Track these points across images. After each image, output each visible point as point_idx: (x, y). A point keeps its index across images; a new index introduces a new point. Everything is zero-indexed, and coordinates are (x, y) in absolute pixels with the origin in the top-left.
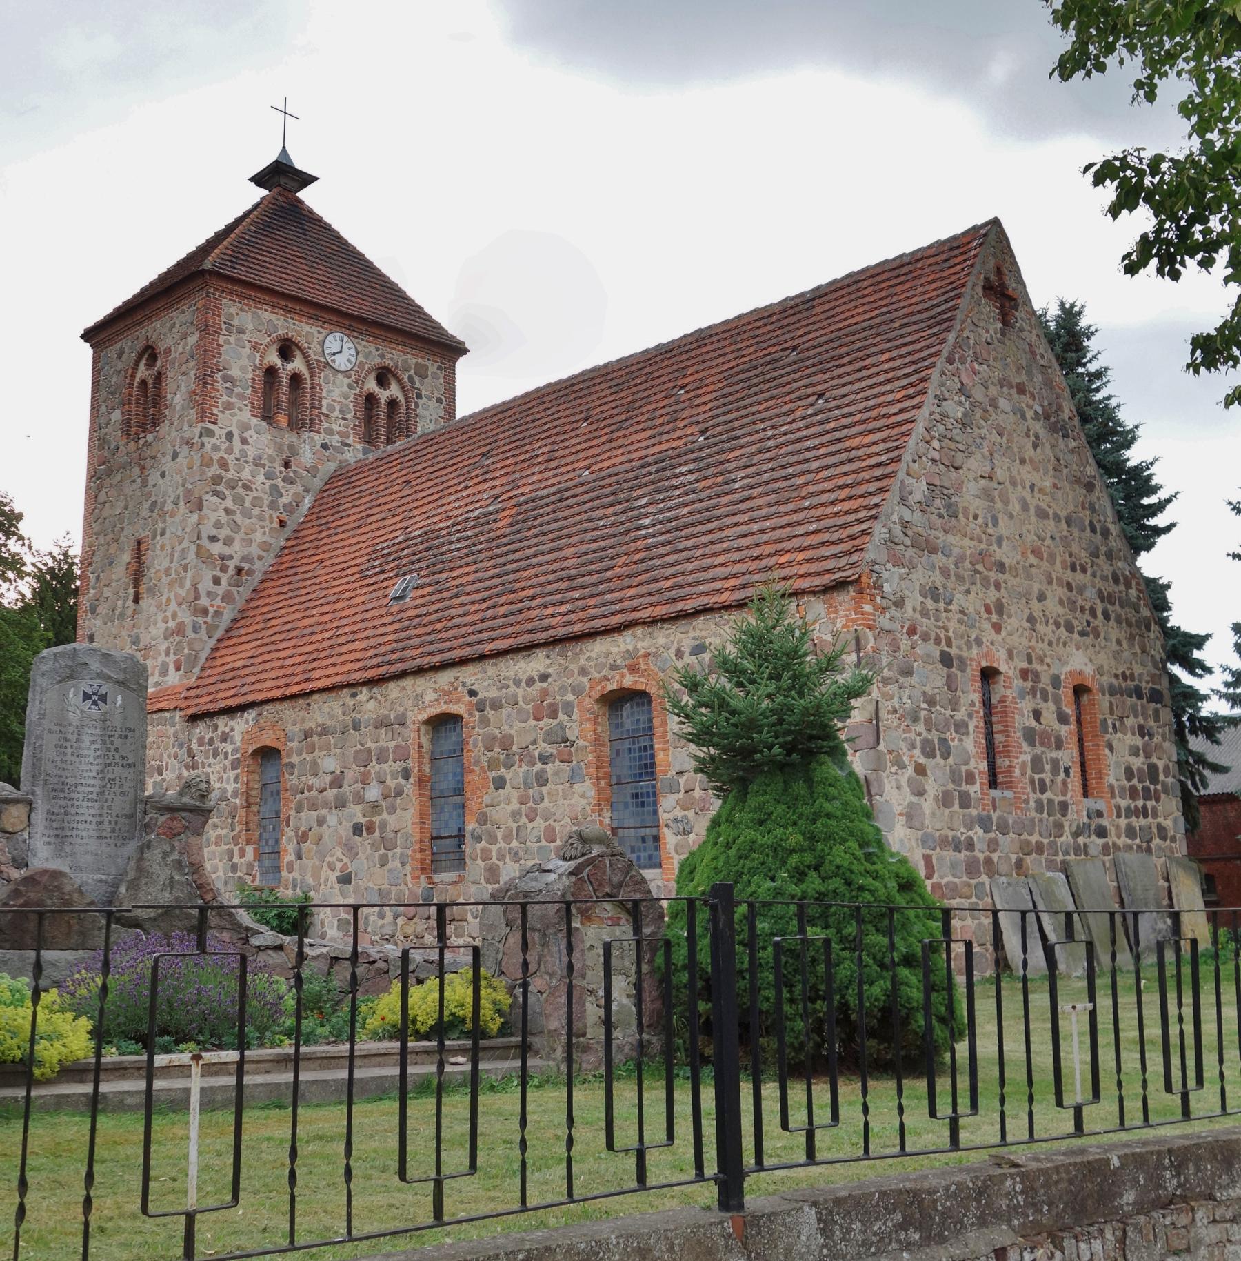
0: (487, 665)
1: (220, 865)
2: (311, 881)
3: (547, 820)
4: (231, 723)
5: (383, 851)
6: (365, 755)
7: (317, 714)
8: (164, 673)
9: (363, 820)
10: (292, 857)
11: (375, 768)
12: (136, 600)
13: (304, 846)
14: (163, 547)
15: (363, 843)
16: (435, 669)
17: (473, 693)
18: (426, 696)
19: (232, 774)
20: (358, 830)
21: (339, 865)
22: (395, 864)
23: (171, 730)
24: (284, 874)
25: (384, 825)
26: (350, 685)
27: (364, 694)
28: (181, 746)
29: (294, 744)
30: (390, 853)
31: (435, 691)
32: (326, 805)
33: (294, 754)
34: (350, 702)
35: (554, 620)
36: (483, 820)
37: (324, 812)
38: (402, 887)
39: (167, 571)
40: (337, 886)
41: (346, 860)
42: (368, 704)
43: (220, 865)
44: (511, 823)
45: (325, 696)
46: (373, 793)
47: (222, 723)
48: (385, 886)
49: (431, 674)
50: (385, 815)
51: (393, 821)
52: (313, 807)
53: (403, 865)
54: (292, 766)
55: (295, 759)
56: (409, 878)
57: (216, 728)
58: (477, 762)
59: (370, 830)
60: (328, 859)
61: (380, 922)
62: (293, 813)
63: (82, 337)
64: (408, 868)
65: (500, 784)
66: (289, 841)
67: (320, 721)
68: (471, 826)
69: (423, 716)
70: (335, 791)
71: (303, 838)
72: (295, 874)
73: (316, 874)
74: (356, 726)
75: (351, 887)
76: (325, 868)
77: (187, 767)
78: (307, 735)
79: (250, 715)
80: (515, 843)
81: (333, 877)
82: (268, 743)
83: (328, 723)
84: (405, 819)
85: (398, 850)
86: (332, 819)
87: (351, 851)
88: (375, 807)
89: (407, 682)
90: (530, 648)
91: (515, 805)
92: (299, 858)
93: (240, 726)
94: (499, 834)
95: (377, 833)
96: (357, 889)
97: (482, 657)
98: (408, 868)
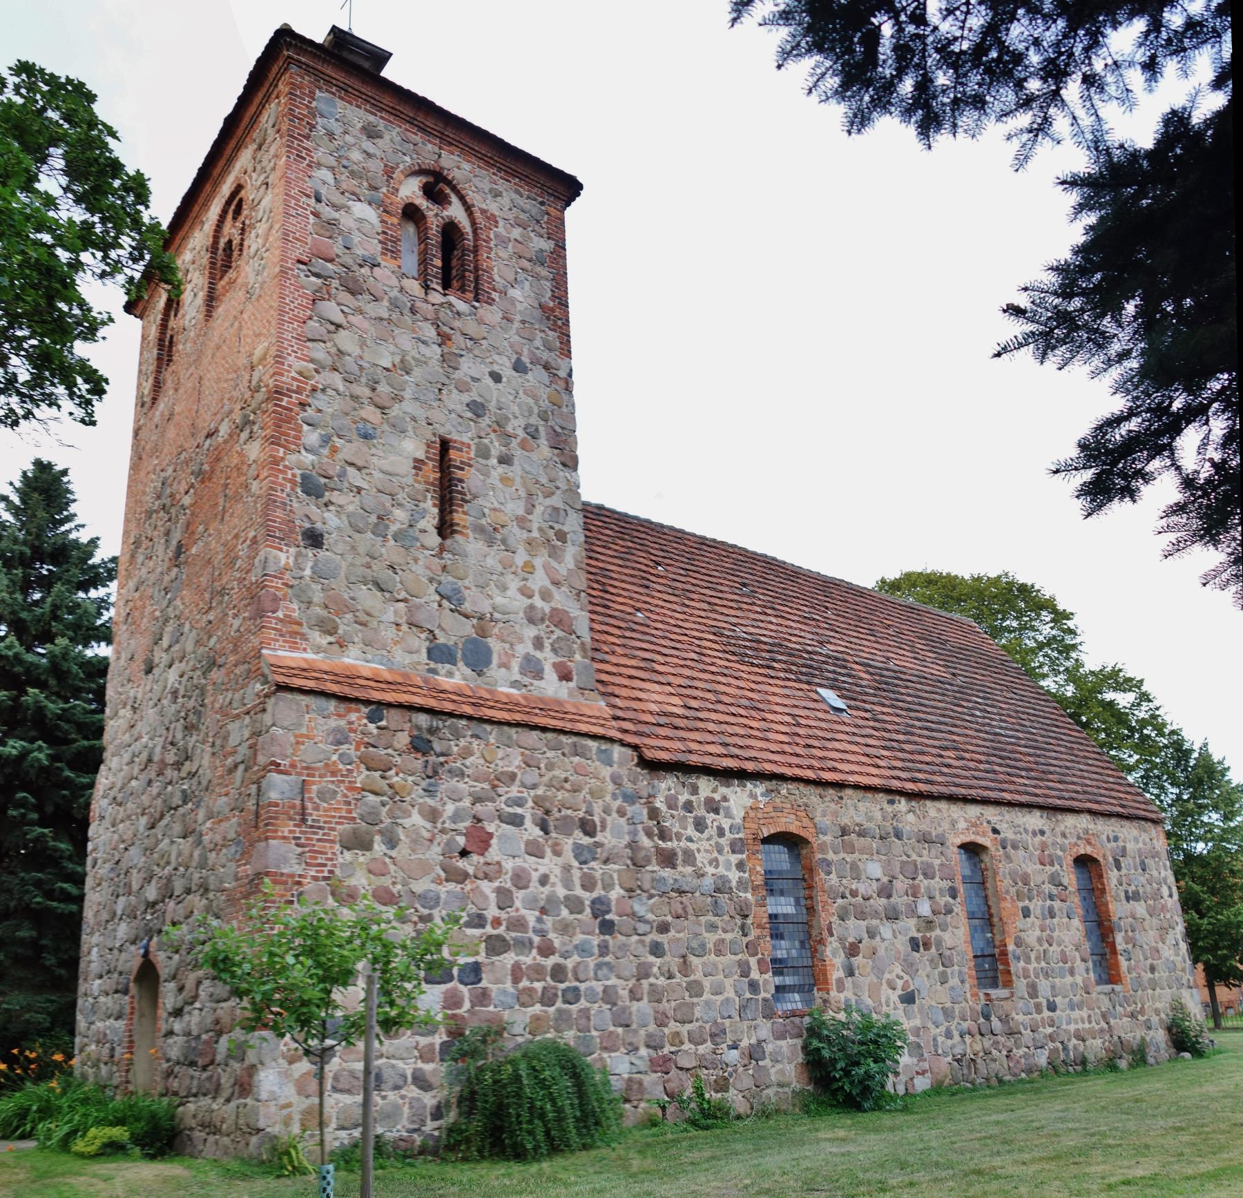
0: (1004, 809)
1: (728, 983)
2: (869, 1002)
3: (1059, 945)
4: (723, 790)
5: (941, 968)
6: (912, 867)
7: (852, 811)
8: (533, 669)
9: (919, 935)
10: (841, 974)
11: (922, 882)
12: (445, 528)
13: (858, 961)
14: (505, 480)
15: (922, 958)
16: (966, 800)
17: (995, 831)
18: (960, 823)
19: (734, 859)
20: (915, 944)
21: (900, 983)
22: (954, 982)
23: (606, 772)
24: (833, 993)
25: (939, 943)
26: (888, 791)
27: (902, 805)
28: (630, 799)
29: (828, 838)
30: (949, 970)
31: (966, 820)
32: (876, 914)
33: (825, 845)
34: (889, 808)
35: (1042, 794)
36: (1019, 943)
37: (875, 922)
38: (964, 1004)
39: (522, 522)
40: (901, 1006)
41: (906, 977)
42: (907, 815)
43: (728, 983)
44: (1038, 947)
45: (860, 794)
46: (925, 908)
47: (706, 786)
48: (948, 1005)
49: (961, 805)
50: (938, 932)
51: (948, 938)
52: (861, 915)
53: (963, 982)
54: (829, 864)
55: (831, 856)
56: (968, 995)
57: (695, 790)
58: (1007, 892)
59: (927, 945)
60: (887, 976)
61: (949, 1042)
62: (834, 919)
63: (334, 27)
64: (967, 985)
65: (1026, 913)
66: (834, 955)
67: (858, 820)
68: (1011, 947)
69: (958, 841)
70: (883, 901)
71: (853, 950)
72: (848, 994)
73: (874, 991)
74: (898, 835)
75: (915, 1007)
76: (885, 986)
77: (649, 834)
78: (844, 831)
79: (760, 788)
80: (1043, 964)
81: (894, 996)
82: (793, 829)
83: (867, 825)
84: (957, 936)
85: (956, 967)
86: (886, 930)
87: (910, 968)
88: (929, 924)
89: (943, 805)
90: (1029, 806)
91: (1038, 933)
92: (851, 973)
93: (739, 798)
94: (1033, 955)
95: (933, 950)
96: (921, 1010)
97: (1010, 804)
98: (967, 985)
